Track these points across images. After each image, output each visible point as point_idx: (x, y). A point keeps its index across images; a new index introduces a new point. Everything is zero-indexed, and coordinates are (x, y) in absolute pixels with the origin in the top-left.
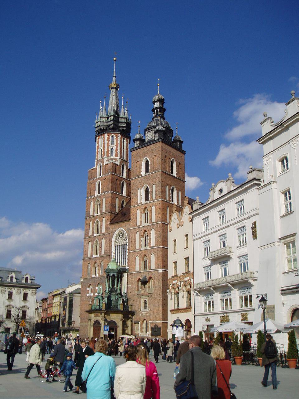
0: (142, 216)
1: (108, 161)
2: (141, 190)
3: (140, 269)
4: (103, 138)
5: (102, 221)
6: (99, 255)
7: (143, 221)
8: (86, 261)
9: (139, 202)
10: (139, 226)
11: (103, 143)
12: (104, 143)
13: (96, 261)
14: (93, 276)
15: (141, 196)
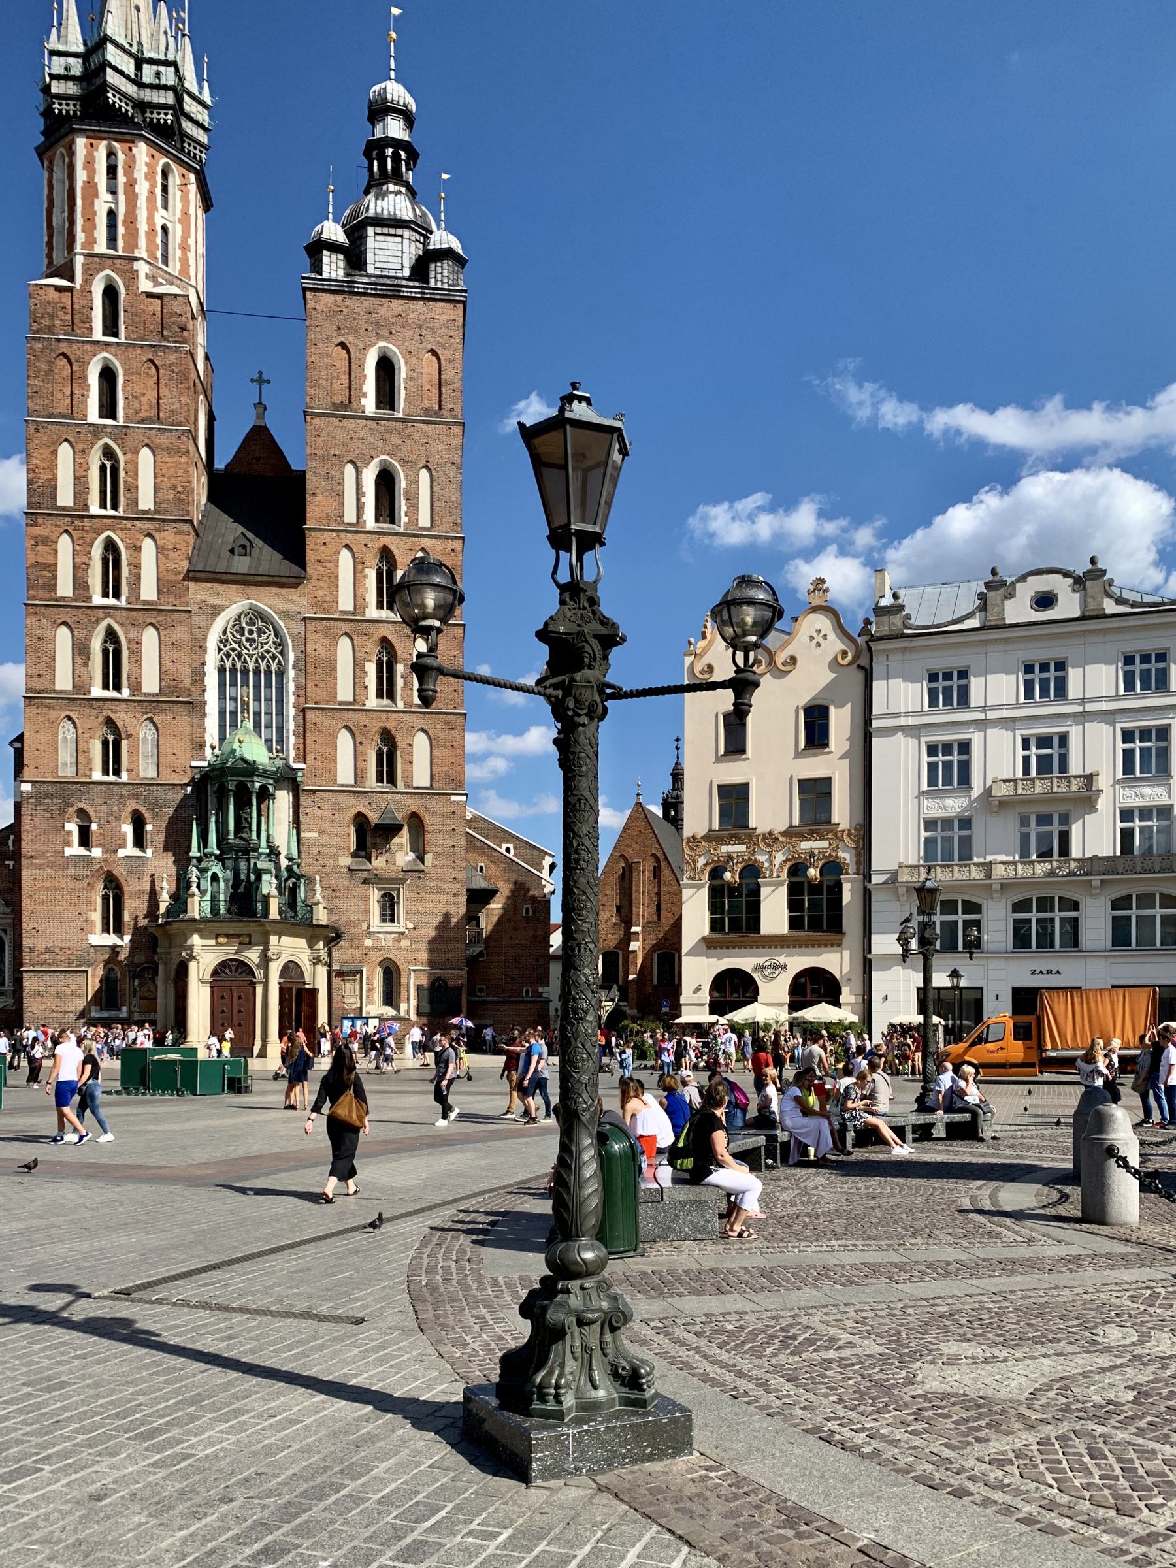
0: (366, 576)
1: (152, 278)
2: (358, 472)
3: (359, 777)
4: (121, 158)
5: (137, 548)
6: (126, 693)
7: (372, 597)
8: (49, 707)
9: (350, 516)
10: (354, 613)
11: (121, 178)
12: (131, 184)
13: (113, 716)
14: (97, 776)
15: (364, 495)
